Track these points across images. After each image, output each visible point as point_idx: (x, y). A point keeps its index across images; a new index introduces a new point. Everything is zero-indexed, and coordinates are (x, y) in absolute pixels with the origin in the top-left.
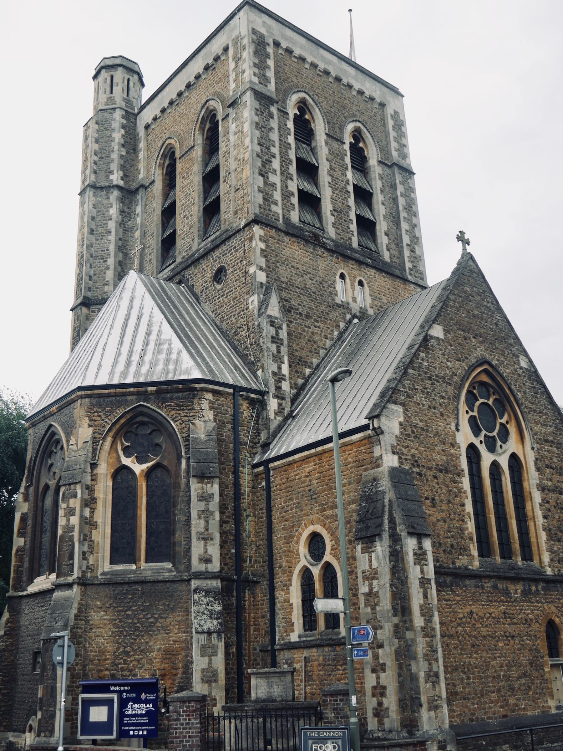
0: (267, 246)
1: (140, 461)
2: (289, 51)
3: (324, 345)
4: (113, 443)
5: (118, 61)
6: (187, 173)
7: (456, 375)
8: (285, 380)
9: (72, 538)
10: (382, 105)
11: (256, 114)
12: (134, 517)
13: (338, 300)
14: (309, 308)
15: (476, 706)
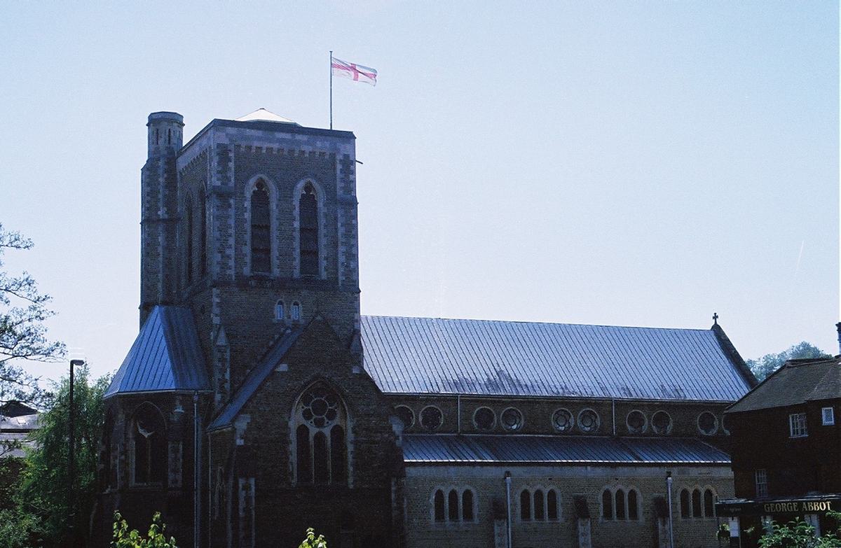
4: (135, 422)
13: (274, 321)
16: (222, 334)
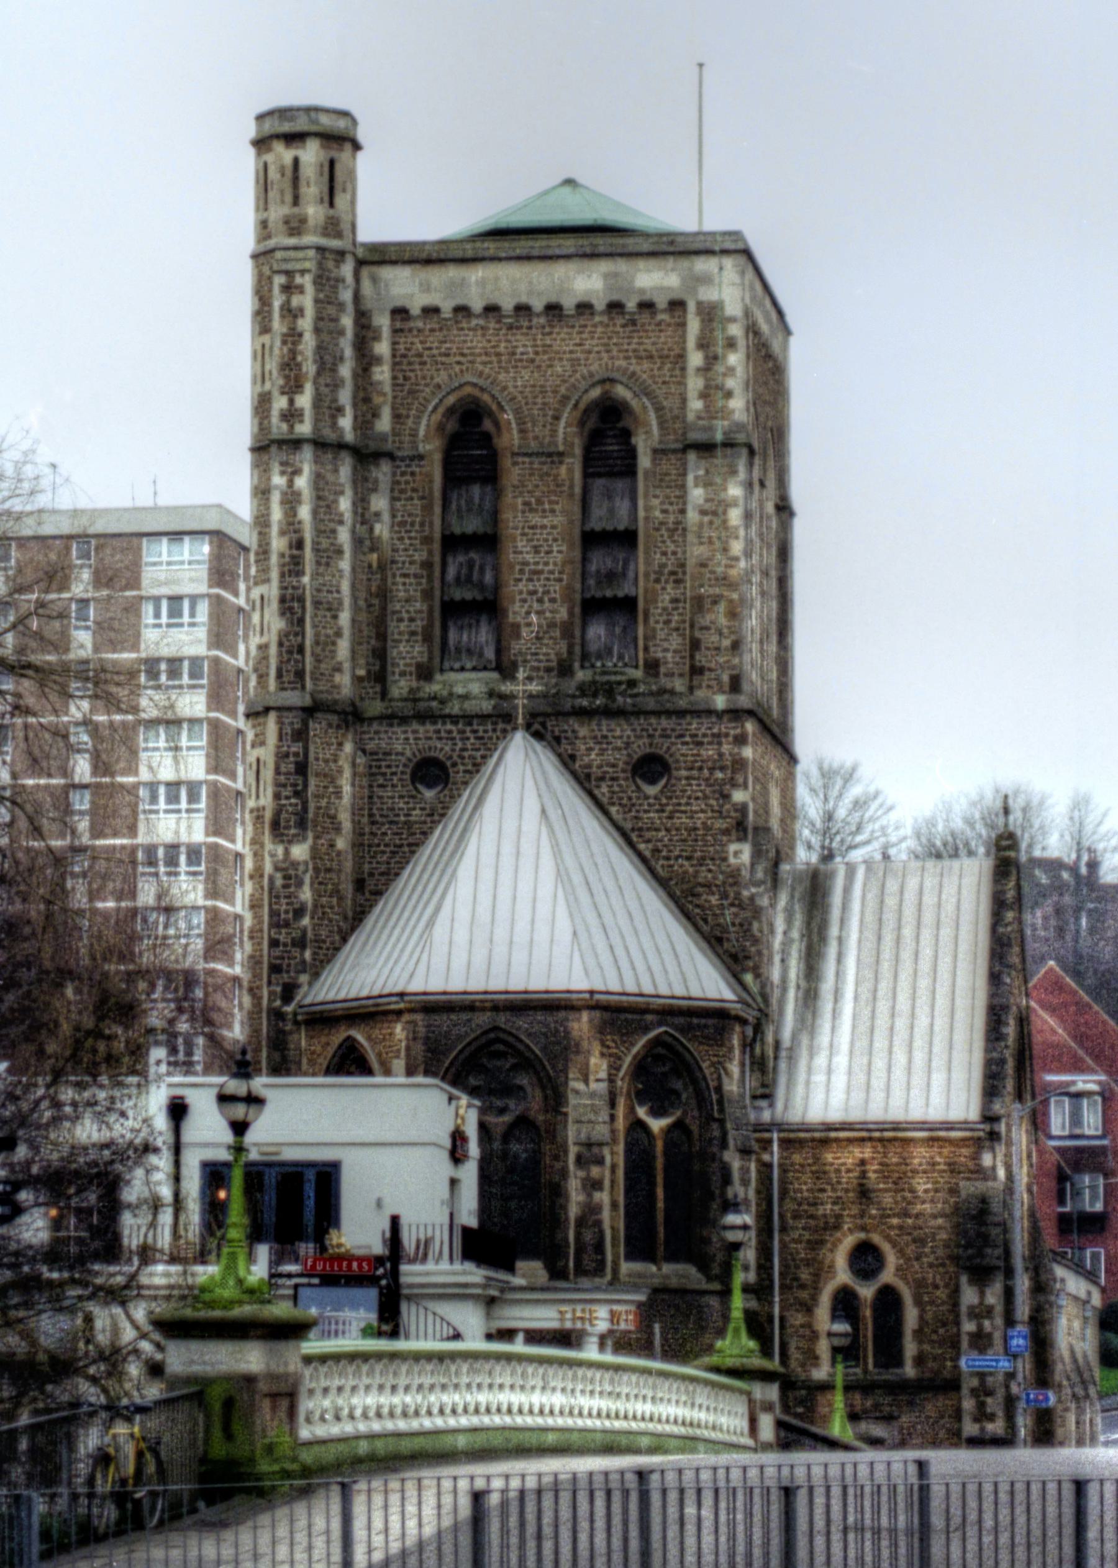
1: (656, 1113)
6: (539, 502)
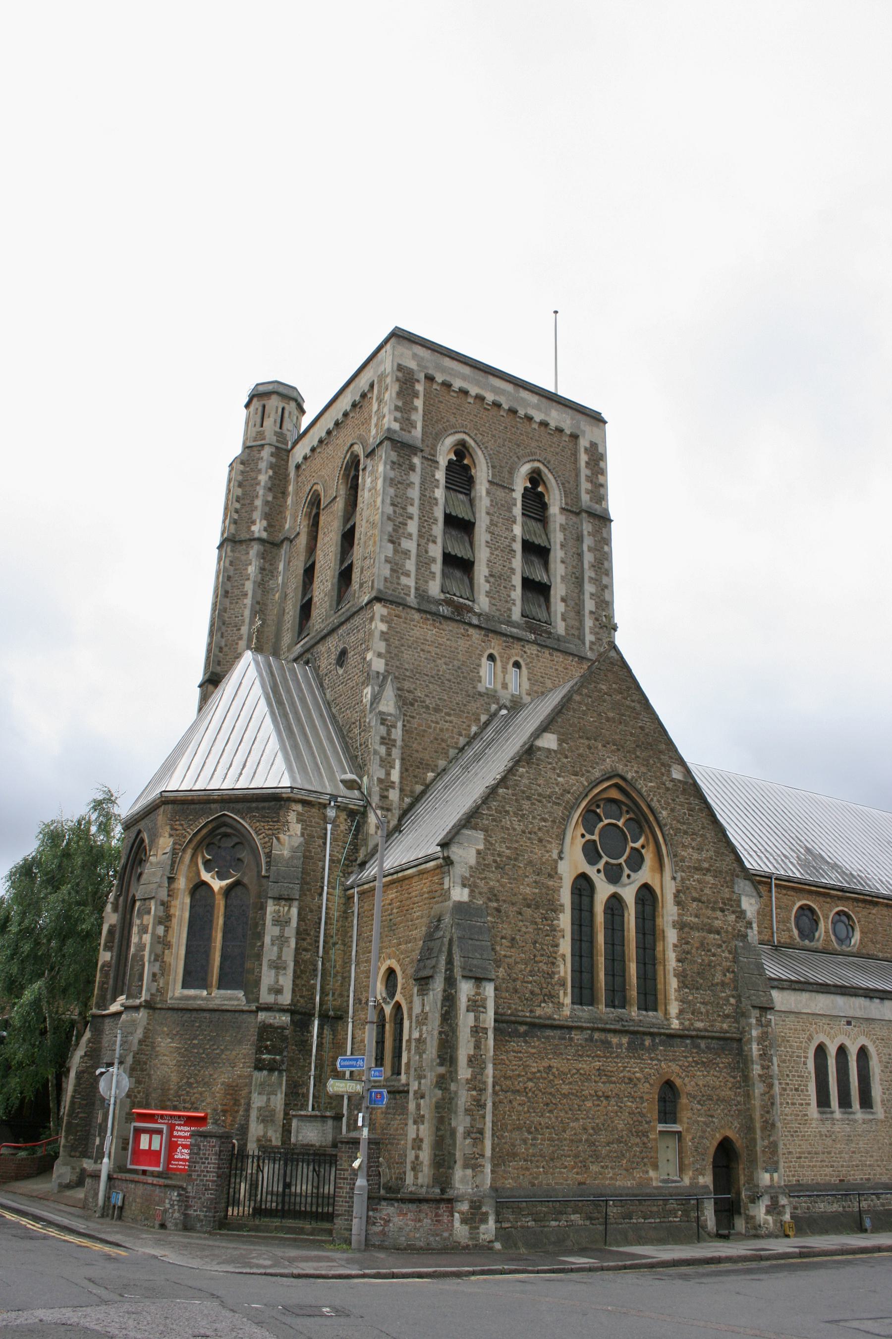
0: (390, 628)
1: (221, 877)
2: (447, 385)
3: (456, 743)
5: (270, 388)
7: (569, 793)
8: (393, 788)
9: (142, 958)
10: (575, 437)
11: (392, 469)
12: (209, 939)
13: (481, 688)
14: (440, 699)
15: (541, 1170)
16: (389, 693)
